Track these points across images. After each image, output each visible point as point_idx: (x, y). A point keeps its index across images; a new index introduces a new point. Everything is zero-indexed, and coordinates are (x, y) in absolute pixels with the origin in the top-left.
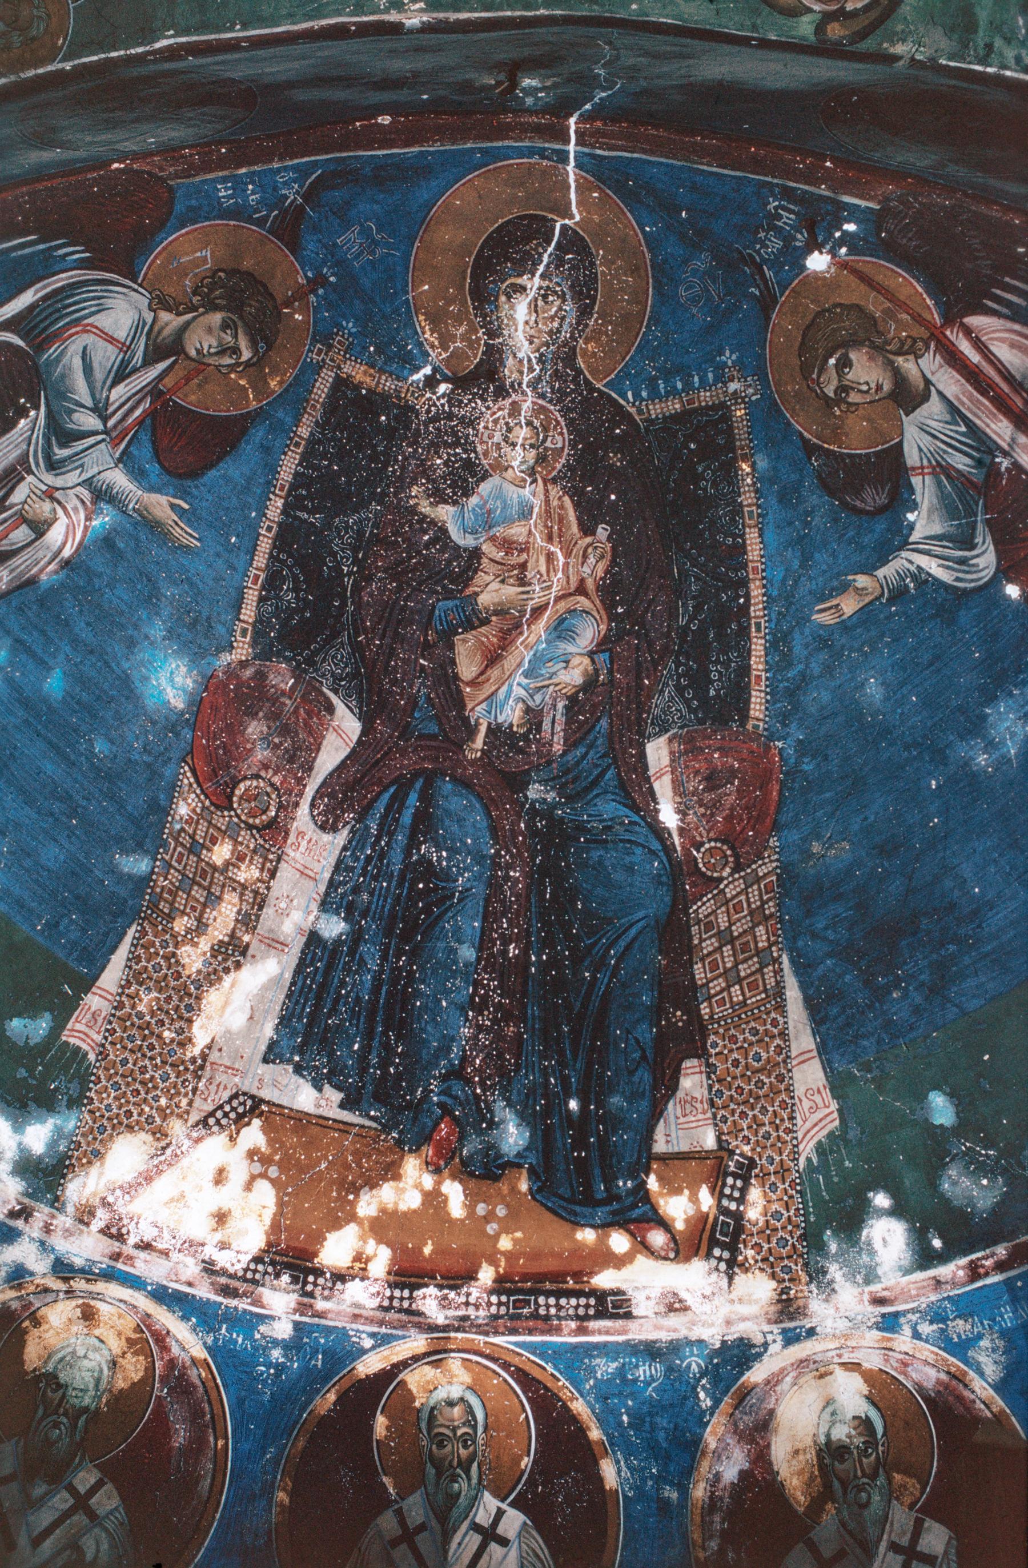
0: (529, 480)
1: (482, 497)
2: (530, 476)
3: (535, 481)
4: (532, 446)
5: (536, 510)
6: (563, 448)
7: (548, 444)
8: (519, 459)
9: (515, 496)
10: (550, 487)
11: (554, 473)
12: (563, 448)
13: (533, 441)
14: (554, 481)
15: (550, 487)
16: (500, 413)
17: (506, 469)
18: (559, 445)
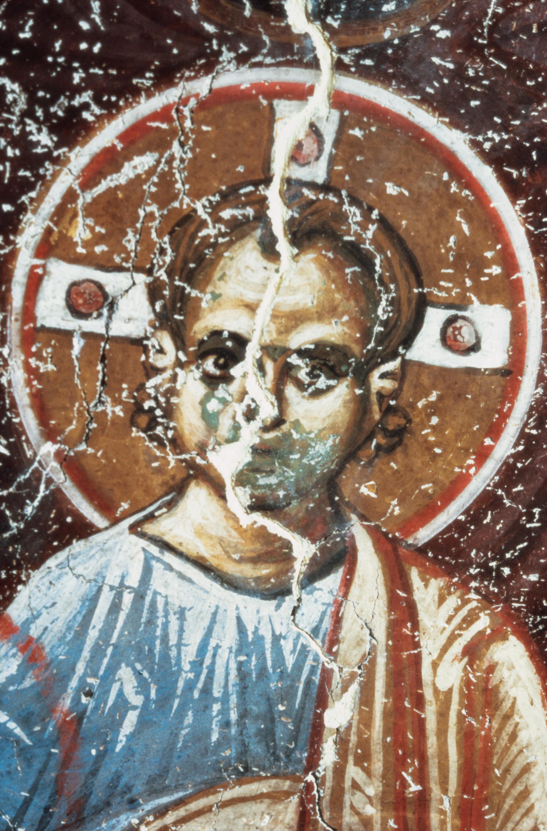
0: (303, 550)
1: (32, 653)
2: (305, 529)
3: (336, 558)
4: (326, 360)
5: (339, 714)
6: (511, 372)
7: (426, 348)
8: (250, 435)
9: (227, 638)
10: (426, 592)
11: (453, 512)
12: (511, 372)
13: (332, 331)
14: (446, 556)
15: (426, 592)
16: (143, 162)
17: (177, 490)
18: (493, 355)
